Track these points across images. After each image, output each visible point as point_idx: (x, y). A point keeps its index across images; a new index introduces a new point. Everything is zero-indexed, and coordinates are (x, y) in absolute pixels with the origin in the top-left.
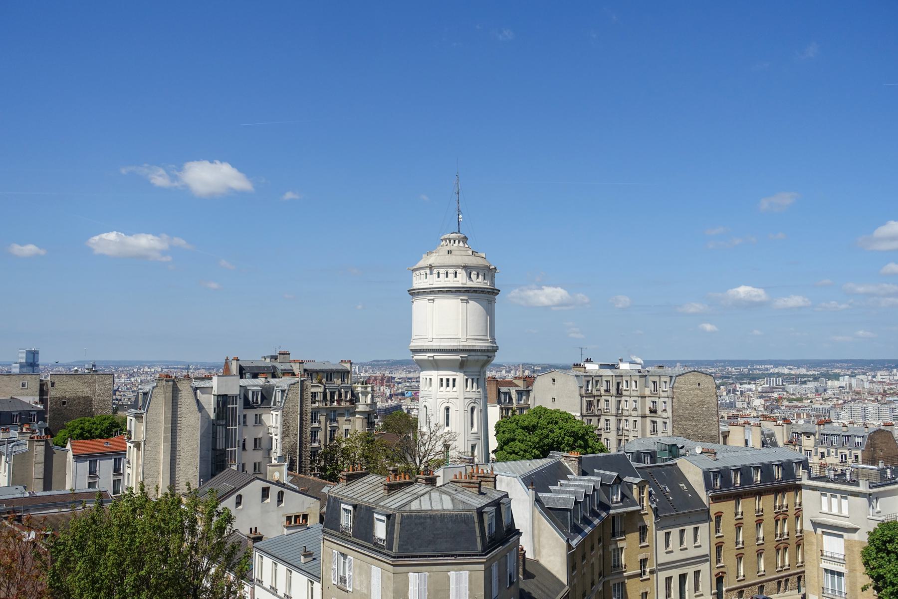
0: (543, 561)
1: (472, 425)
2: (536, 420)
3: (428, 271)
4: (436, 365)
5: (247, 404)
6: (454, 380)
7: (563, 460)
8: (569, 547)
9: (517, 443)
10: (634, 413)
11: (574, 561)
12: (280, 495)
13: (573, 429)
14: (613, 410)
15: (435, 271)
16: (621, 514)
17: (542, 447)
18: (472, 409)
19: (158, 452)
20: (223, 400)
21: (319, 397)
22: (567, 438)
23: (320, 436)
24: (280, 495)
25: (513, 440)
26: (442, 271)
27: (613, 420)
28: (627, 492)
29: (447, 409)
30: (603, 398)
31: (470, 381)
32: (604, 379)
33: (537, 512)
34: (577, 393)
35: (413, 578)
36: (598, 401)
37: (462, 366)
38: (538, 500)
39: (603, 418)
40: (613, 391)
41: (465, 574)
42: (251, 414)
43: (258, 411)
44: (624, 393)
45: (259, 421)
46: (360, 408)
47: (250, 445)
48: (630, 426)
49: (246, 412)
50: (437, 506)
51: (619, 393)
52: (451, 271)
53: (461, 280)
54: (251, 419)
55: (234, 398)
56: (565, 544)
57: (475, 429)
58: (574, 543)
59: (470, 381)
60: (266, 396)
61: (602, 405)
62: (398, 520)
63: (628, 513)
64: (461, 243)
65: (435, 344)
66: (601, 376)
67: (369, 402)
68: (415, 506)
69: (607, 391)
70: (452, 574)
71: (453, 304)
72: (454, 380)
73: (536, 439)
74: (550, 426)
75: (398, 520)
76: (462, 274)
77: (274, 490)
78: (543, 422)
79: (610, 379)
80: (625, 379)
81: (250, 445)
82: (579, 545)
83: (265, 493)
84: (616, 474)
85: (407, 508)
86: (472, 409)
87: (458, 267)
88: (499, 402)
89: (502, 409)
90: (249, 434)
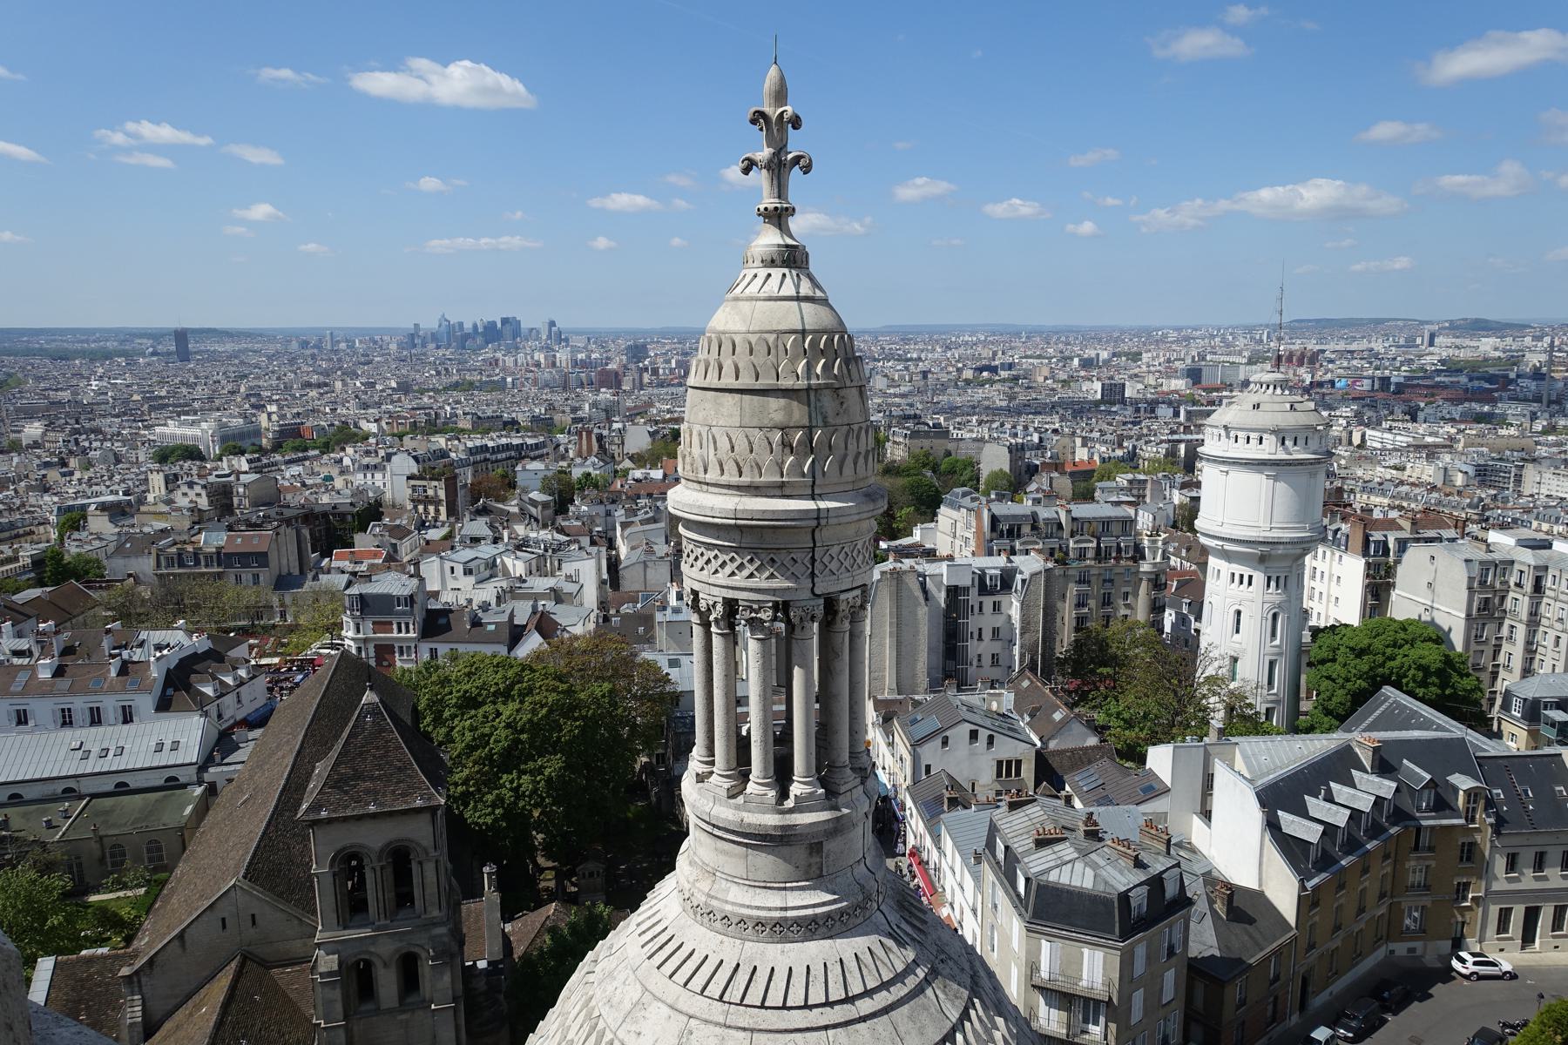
0: (1268, 894)
1: (1273, 634)
2: (1366, 641)
3: (1223, 433)
4: (1227, 556)
5: (984, 589)
6: (1250, 577)
7: (1354, 744)
8: (1303, 888)
9: (1337, 667)
10: (1558, 626)
11: (1307, 903)
12: (991, 740)
13: (1423, 662)
14: (1524, 616)
15: (1232, 434)
16: (1432, 828)
17: (1373, 678)
18: (1275, 616)
19: (882, 645)
20: (953, 591)
21: (1090, 554)
22: (1412, 672)
23: (1092, 603)
24: (991, 740)
25: (1334, 660)
26: (1242, 435)
27: (1521, 631)
28: (1448, 798)
29: (1239, 613)
30: (1511, 595)
31: (1273, 584)
32: (1517, 567)
33: (1268, 836)
34: (1465, 585)
35: (1045, 946)
36: (1503, 598)
37: (1262, 560)
38: (1272, 825)
39: (1507, 622)
40: (1528, 586)
41: (1099, 955)
42: (988, 601)
43: (997, 598)
44: (1548, 592)
45: (997, 607)
46: (1145, 567)
47: (987, 635)
48: (1549, 642)
49: (982, 598)
50: (1076, 882)
51: (1538, 587)
52: (1252, 435)
53: (1269, 449)
54: (988, 607)
55: (966, 590)
56: (1297, 884)
57: (1277, 642)
58: (1309, 885)
59: (1273, 584)
60: (1006, 580)
61: (1508, 604)
62: (1034, 887)
63: (1442, 827)
64: (1279, 391)
65: (1226, 531)
66: (1512, 562)
67: (1158, 559)
68: (1053, 877)
69: (1518, 585)
70: (1086, 951)
71: (1258, 482)
72: (1250, 577)
73: (1365, 668)
74: (1389, 651)
75: (1034, 887)
76: (1270, 441)
77: (983, 734)
78: (1378, 644)
79: (1525, 569)
80: (1551, 572)
81: (987, 635)
82: (1316, 888)
83: (974, 735)
84: (1428, 777)
85: (1044, 878)
86: (1275, 616)
87: (1264, 431)
88: (1365, 553)
89: (1368, 565)
90: (987, 621)
